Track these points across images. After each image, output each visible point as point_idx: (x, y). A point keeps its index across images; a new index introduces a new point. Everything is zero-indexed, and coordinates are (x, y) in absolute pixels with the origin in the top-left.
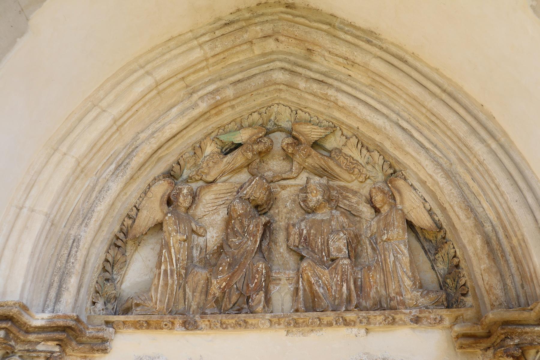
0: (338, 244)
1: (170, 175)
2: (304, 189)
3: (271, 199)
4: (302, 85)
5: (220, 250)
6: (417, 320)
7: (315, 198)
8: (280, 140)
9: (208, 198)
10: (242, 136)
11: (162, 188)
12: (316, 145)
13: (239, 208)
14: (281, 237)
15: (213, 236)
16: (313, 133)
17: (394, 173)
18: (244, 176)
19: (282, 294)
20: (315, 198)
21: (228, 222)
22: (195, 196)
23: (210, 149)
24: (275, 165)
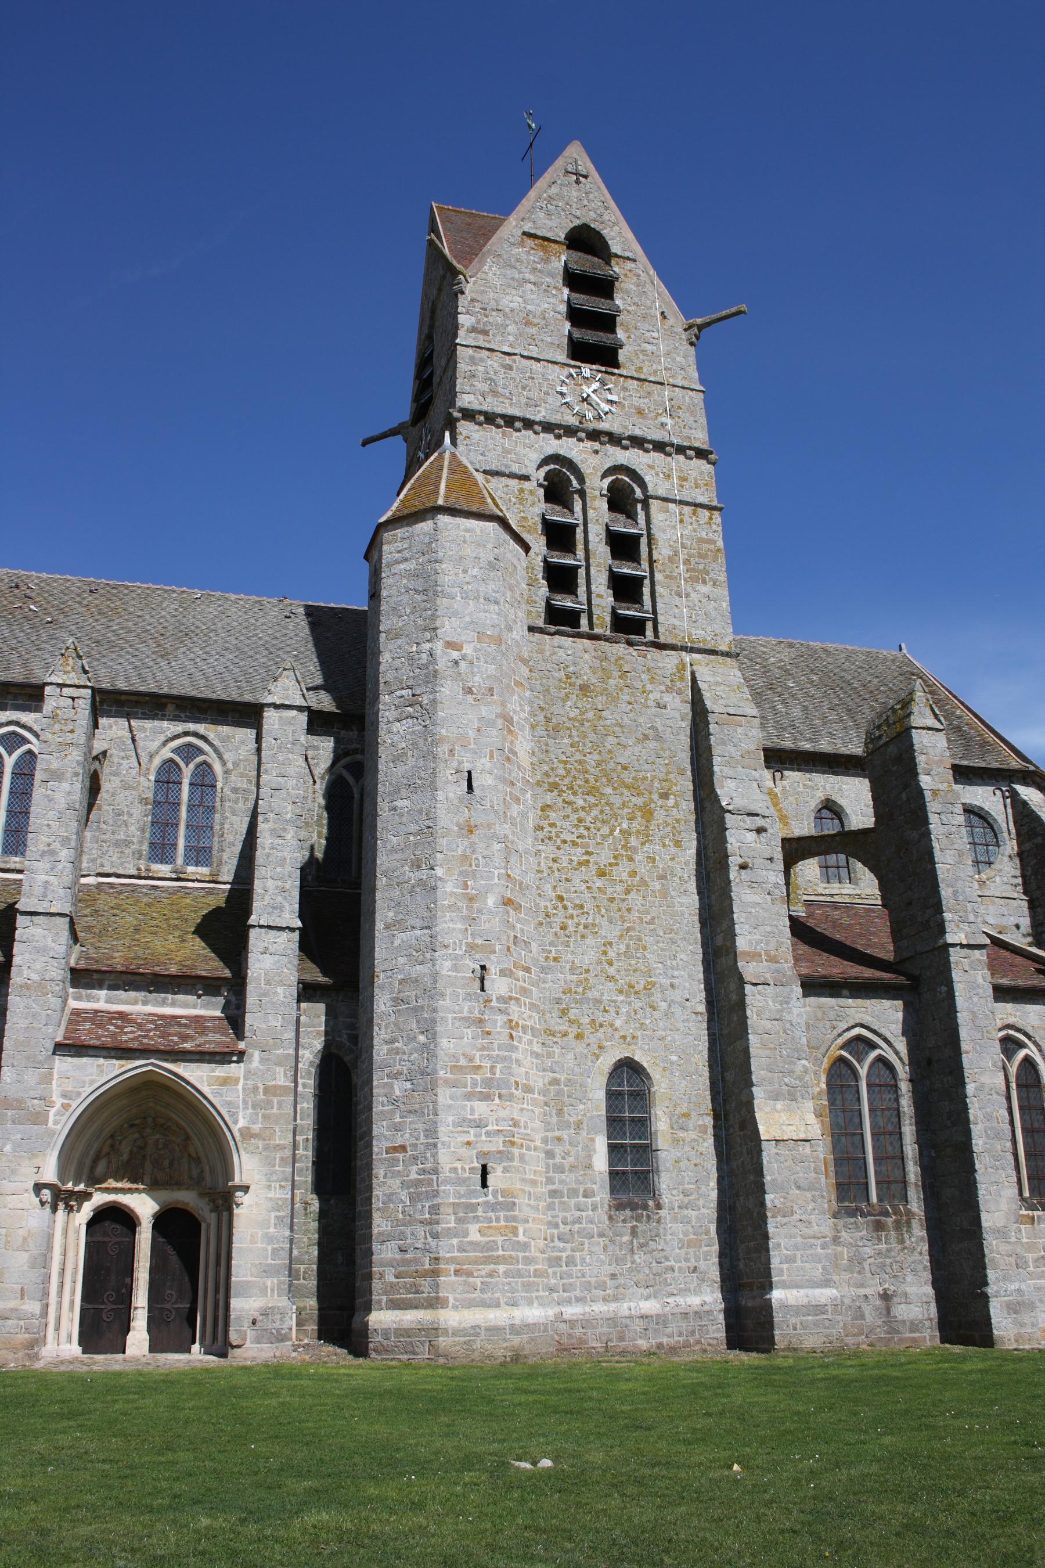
0: (166, 1163)
1: (112, 1136)
2: (157, 1140)
3: (146, 1144)
4: (158, 1108)
5: (129, 1161)
6: (187, 1189)
7: (160, 1146)
8: (150, 1120)
9: (124, 1143)
10: (137, 1122)
11: (109, 1142)
12: (162, 1125)
13: (135, 1149)
14: (148, 1157)
15: (125, 1157)
16: (162, 1121)
17: (188, 1138)
18: (137, 1135)
19: (147, 1179)
20: (160, 1146)
21: (131, 1152)
22: (120, 1143)
23: (126, 1126)
24: (148, 1131)
